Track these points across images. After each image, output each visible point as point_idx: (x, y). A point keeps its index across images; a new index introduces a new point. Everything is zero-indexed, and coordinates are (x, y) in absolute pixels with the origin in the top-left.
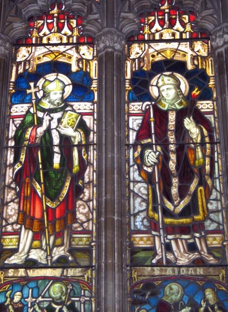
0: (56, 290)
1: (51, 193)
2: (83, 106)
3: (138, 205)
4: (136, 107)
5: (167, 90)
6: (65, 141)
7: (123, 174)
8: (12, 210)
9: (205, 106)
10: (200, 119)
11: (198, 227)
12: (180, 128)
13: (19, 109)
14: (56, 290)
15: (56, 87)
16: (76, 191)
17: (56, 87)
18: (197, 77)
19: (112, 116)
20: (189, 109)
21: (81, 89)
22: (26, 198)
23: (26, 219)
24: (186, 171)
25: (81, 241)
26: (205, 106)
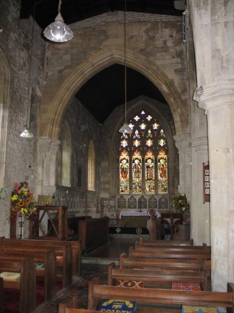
0: (125, 184)
1: (125, 174)
2: (127, 164)
3: (133, 175)
4: (133, 164)
5: (137, 162)
6: (126, 168)
7: (132, 172)
8: (121, 176)
9: (141, 164)
10: (140, 165)
11: (139, 178)
12: (138, 167)
13: (121, 164)
14: (125, 184)
15: (124, 161)
16: (127, 174)
17: (124, 161)
18: (140, 160)
19: (131, 165)
20: (139, 164)
21: (127, 162)
22: (122, 174)
23: (122, 177)
24: (138, 172)
25: (128, 179)
26: (141, 164)
